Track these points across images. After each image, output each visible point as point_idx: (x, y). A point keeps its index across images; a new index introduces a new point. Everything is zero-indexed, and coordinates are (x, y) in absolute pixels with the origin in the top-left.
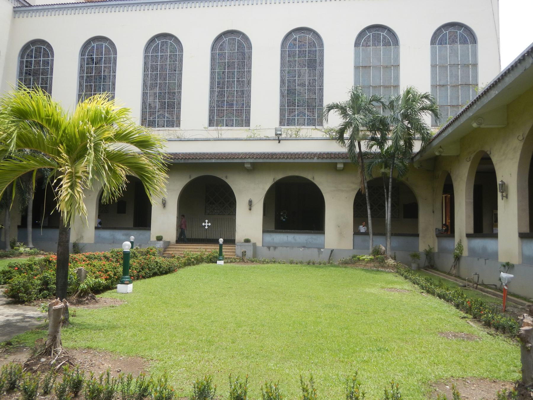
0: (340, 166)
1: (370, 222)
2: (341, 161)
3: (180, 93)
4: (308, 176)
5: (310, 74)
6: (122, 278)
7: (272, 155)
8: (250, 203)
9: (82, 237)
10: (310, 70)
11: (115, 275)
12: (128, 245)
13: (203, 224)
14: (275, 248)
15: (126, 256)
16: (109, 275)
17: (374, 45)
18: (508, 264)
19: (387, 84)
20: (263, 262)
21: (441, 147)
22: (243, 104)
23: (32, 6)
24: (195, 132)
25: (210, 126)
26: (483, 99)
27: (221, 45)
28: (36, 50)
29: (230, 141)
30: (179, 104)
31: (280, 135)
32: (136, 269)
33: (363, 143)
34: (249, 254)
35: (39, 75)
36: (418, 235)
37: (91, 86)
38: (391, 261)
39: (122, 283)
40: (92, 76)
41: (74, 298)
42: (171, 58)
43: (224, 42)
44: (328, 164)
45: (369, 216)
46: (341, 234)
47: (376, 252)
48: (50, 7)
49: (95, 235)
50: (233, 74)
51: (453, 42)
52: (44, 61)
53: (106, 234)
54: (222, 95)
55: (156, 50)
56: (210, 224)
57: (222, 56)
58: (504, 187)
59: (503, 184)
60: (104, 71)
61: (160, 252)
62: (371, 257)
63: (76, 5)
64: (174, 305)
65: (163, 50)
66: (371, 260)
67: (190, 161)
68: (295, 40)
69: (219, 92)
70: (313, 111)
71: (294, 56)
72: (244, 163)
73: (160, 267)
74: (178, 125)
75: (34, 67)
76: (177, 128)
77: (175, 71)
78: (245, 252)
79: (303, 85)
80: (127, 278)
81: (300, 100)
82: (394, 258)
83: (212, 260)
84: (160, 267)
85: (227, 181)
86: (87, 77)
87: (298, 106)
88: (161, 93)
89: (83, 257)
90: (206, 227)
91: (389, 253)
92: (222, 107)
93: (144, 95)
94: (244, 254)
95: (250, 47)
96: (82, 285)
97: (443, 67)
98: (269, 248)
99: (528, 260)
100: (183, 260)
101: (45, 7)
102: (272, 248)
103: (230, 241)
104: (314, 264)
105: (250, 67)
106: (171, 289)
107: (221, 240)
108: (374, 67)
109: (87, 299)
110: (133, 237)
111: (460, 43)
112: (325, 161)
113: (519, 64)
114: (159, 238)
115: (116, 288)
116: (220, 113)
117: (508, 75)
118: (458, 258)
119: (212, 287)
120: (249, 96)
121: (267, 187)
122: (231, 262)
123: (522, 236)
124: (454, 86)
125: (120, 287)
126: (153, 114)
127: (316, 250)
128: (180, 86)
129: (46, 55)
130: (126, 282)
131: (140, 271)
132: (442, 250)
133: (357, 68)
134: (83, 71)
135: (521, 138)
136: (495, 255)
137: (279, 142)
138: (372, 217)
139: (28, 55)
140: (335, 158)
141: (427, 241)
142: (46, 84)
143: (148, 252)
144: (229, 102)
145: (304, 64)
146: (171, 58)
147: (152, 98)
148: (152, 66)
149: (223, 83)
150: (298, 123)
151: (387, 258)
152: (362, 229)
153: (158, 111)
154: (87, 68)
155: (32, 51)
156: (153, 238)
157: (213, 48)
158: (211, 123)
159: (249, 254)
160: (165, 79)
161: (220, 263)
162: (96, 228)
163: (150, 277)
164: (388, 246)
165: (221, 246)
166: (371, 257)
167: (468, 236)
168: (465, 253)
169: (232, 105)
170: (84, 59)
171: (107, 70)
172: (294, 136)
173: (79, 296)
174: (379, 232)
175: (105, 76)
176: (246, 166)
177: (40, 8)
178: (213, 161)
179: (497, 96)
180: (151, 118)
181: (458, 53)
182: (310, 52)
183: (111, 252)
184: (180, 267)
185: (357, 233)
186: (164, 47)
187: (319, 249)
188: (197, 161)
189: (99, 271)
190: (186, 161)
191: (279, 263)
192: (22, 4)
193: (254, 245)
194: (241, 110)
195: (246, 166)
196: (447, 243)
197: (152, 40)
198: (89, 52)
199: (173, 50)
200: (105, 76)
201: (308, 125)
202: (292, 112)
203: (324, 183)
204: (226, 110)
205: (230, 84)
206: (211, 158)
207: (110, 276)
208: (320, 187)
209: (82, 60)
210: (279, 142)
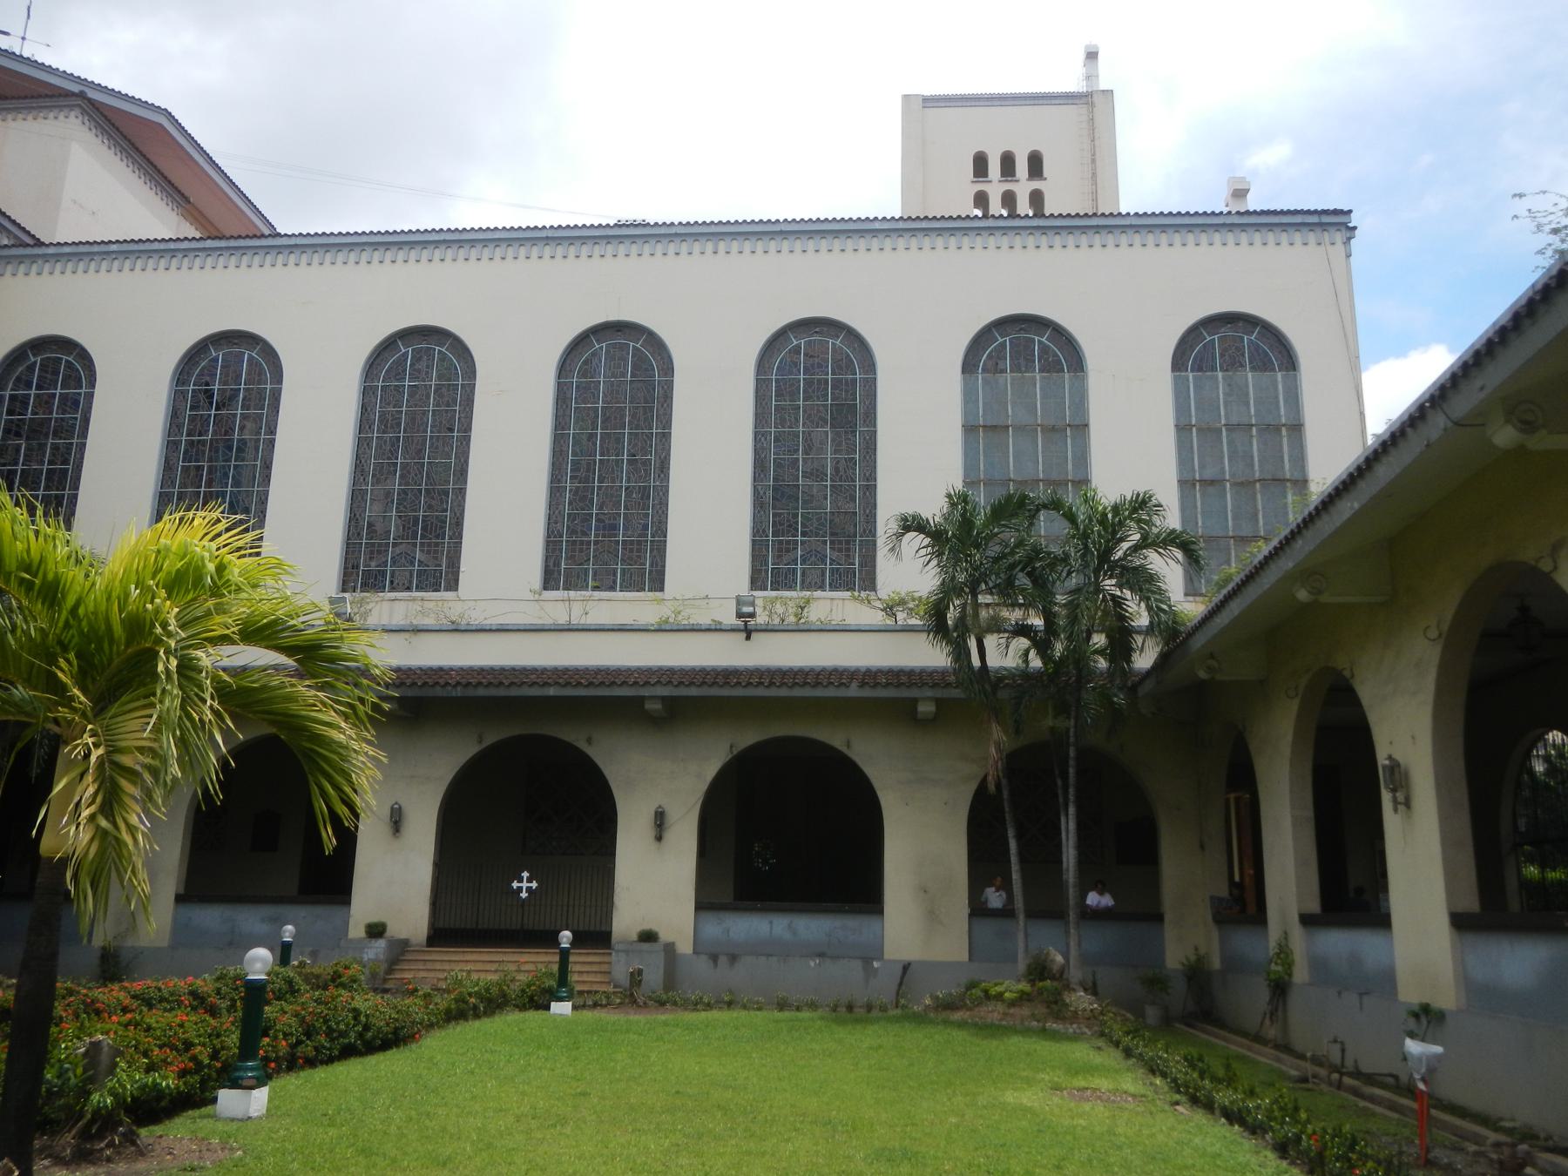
0: (926, 708)
1: (1016, 876)
2: (929, 693)
3: (461, 492)
4: (833, 736)
5: (840, 444)
6: (237, 1069)
7: (728, 676)
8: (660, 821)
9: (133, 927)
10: (838, 434)
11: (214, 1056)
12: (262, 960)
13: (515, 885)
14: (733, 958)
15: (255, 994)
16: (194, 1058)
17: (1016, 368)
18: (1426, 1009)
19: (1055, 476)
20: (696, 1005)
21: (1212, 656)
22: (645, 527)
23: (39, 243)
24: (502, 606)
25: (545, 588)
26: (1319, 524)
27: (586, 363)
28: (43, 368)
29: (606, 634)
30: (458, 524)
31: (752, 615)
32: (285, 1035)
33: (991, 641)
34: (654, 978)
35: (47, 436)
36: (1159, 918)
37: (199, 468)
38: (1080, 1000)
39: (235, 1084)
40: (203, 443)
41: (67, 1141)
42: (441, 396)
43: (593, 354)
44: (889, 700)
45: (1014, 859)
46: (932, 916)
47: (1039, 970)
48: (96, 249)
49: (175, 920)
50: (619, 440)
51: (1233, 363)
52: (64, 398)
53: (210, 917)
54: (583, 498)
55: (397, 372)
56: (534, 885)
57: (587, 391)
58: (1399, 777)
59: (1394, 767)
60: (242, 428)
61: (374, 976)
62: (1024, 986)
63: (172, 246)
64: (394, 1160)
65: (419, 371)
66: (1024, 998)
67: (481, 692)
68: (797, 350)
69: (575, 492)
70: (848, 550)
71: (794, 395)
73: (367, 1028)
74: (453, 585)
75: (34, 413)
76: (450, 595)
77: (451, 430)
78: (640, 972)
79: (818, 474)
80: (252, 1069)
81: (811, 517)
82: (1093, 989)
83: (537, 1000)
84: (367, 1028)
85: (592, 752)
86: (191, 444)
87: (804, 534)
88: (405, 492)
89: (122, 995)
90: (524, 895)
91: (1075, 974)
92: (585, 534)
93: (357, 497)
94: (636, 978)
95: (668, 368)
96: (95, 1097)
97: (1209, 432)
98: (714, 958)
99: (1484, 997)
100: (443, 1002)
101: (82, 249)
102: (723, 960)
103: (596, 937)
104: (850, 1008)
105: (667, 424)
106: (394, 1101)
107: (566, 936)
108: (1019, 429)
109: (111, 1145)
110: (290, 927)
111: (1253, 369)
112: (881, 693)
113: (1409, 430)
114: (376, 931)
115: (214, 1100)
116: (578, 549)
117: (1384, 460)
118: (1280, 989)
119: (524, 1093)
120: (663, 504)
121: (711, 770)
122: (595, 1005)
123: (1461, 922)
124: (1242, 484)
125: (228, 1099)
126: (379, 552)
127: (857, 965)
128: (462, 473)
129: (73, 379)
130: (245, 1083)
131: (299, 1042)
132: (1234, 965)
133: (969, 429)
134: (180, 427)
135: (1433, 633)
136: (1386, 981)
137: (748, 638)
138: (1023, 860)
139: (18, 379)
140: (910, 685)
141: (1186, 938)
142: (66, 462)
143: (336, 977)
144: (606, 522)
145: (821, 418)
146: (441, 396)
147: (378, 507)
148: (382, 414)
149: (590, 467)
150: (803, 582)
151: (1068, 987)
152: (994, 898)
153: (395, 545)
154: (192, 419)
155: (31, 368)
156: (357, 931)
157: (564, 368)
158: (550, 579)
159: (654, 978)
161: (561, 1008)
162: (180, 899)
163: (330, 1060)
164: (1073, 952)
165: (564, 954)
166: (1024, 986)
167: (1307, 920)
168: (1300, 975)
169: (615, 527)
170: (184, 393)
171: (249, 425)
172: (792, 619)
173: (85, 1135)
174: (1046, 905)
175: (242, 442)
176: (648, 706)
177: (67, 250)
178: (552, 692)
179: (1357, 515)
180: (373, 564)
181: (1247, 394)
182: (837, 384)
183: (218, 979)
184: (431, 1026)
185: (978, 910)
186: (422, 365)
187: (867, 961)
188: (502, 692)
189: (161, 1047)
190: (471, 692)
191: (745, 1007)
192: (16, 237)
193: (670, 949)
194: (639, 543)
195: (648, 706)
196: (1244, 941)
197: (388, 345)
198: (201, 374)
199: (447, 373)
200: (242, 442)
201: (834, 587)
202: (788, 551)
203: (881, 760)
204: (596, 543)
206: (546, 684)
207: (199, 1065)
208: (870, 771)
210: (748, 638)
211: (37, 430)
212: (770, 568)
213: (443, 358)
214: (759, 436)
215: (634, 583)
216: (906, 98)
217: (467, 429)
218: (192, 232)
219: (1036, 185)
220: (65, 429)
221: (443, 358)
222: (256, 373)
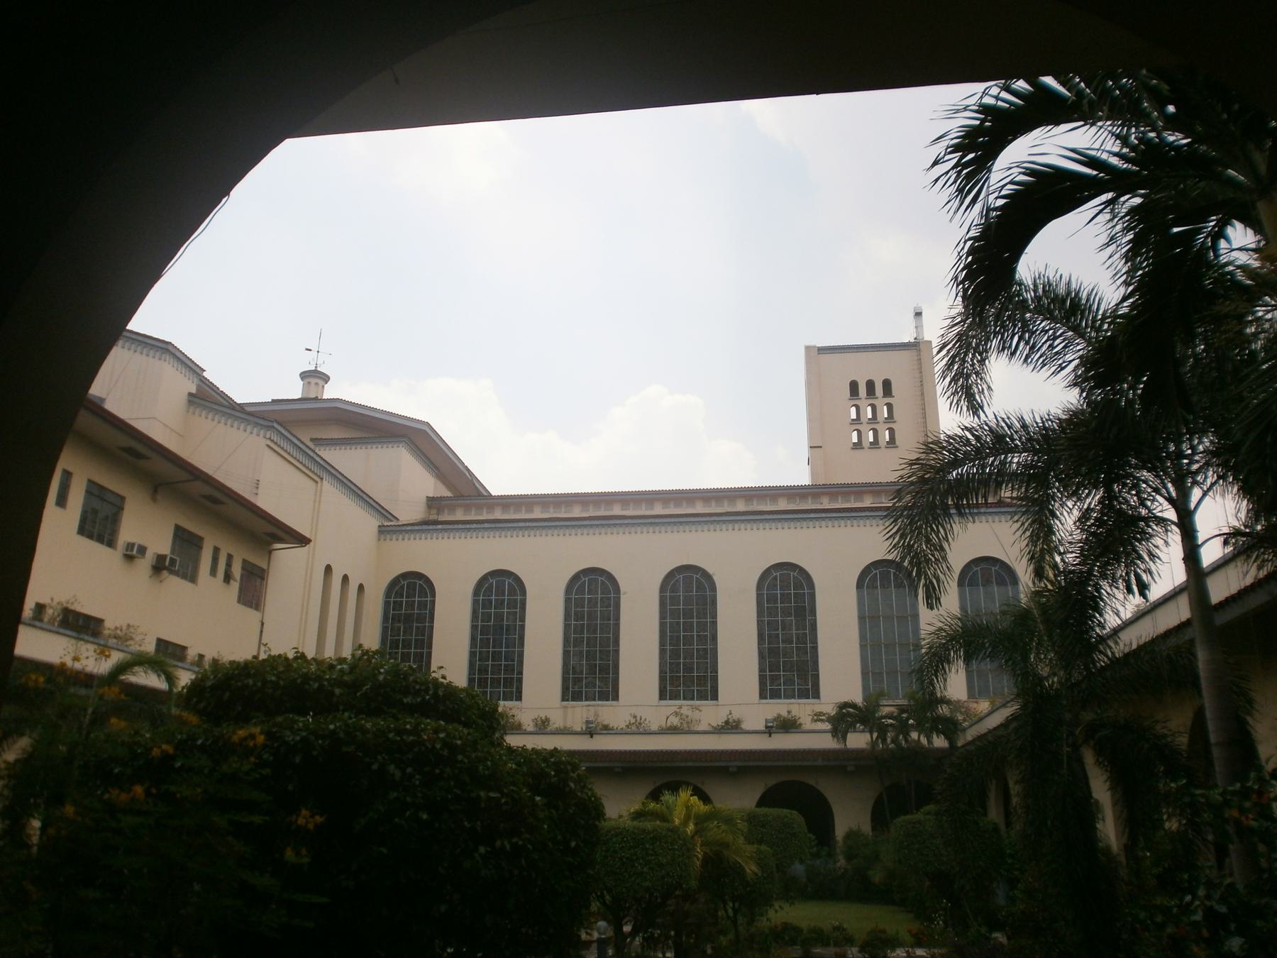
3: (617, 652)
17: (883, 586)
51: (987, 582)
55: (581, 590)
57: (675, 600)
68: (775, 578)
72: (727, 768)
74: (616, 698)
76: (614, 703)
79: (788, 640)
81: (788, 665)
93: (566, 654)
105: (714, 616)
129: (423, 593)
148: (576, 613)
160: (595, 632)
178: (690, 764)
197: (576, 577)
199: (605, 591)
201: (799, 697)
205: (688, 641)
209: (475, 602)
211: (408, 619)
212: (768, 689)
213: (603, 583)
214: (760, 623)
215: (702, 697)
216: (808, 348)
217: (617, 618)
218: (444, 492)
219: (888, 400)
220: (421, 619)
221: (603, 583)
222: (512, 591)
